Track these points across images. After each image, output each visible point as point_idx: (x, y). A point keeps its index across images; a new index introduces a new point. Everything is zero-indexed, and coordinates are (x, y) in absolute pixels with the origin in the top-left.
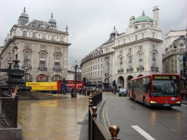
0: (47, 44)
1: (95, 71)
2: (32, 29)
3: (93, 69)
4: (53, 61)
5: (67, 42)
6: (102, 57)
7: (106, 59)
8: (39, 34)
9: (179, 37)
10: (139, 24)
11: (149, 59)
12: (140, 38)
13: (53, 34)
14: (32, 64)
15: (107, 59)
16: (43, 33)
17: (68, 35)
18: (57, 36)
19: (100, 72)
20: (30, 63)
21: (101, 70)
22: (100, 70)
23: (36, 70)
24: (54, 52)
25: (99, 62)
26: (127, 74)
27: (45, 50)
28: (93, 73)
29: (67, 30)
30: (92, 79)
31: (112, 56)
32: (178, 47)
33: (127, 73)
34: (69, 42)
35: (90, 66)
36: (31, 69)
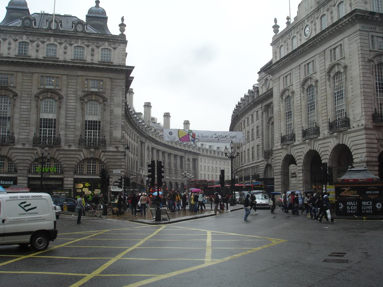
0: (62, 72)
4: (79, 118)
5: (121, 63)
8: (38, 46)
11: (364, 86)
14: (16, 131)
17: (125, 42)
18: (90, 48)
20: (12, 126)
23: (27, 146)
24: (80, 94)
26: (302, 146)
33: (304, 143)
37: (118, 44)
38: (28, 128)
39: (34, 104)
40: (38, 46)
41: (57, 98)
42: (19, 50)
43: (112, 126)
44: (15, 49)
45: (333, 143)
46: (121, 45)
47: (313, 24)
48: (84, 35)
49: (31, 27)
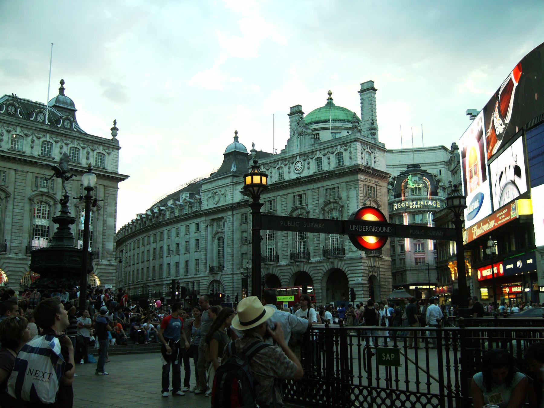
1: (173, 260)
2: (10, 124)
3: (165, 255)
5: (114, 170)
6: (198, 220)
7: (212, 225)
9: (406, 169)
10: (327, 128)
12: (329, 164)
13: (76, 142)
14: (8, 237)
15: (215, 224)
16: (43, 139)
17: (118, 148)
19: (192, 265)
21: (197, 255)
22: (193, 256)
23: (20, 256)
25: (187, 232)
27: (48, 193)
28: (165, 267)
29: (114, 135)
30: (162, 285)
31: (233, 215)
32: (406, 195)
34: (121, 171)
35: (153, 246)
36: (5, 251)
37: (111, 149)
38: (21, 235)
39: (27, 208)
40: (33, 141)
41: (52, 203)
42: (12, 144)
43: (105, 237)
44: (8, 142)
45: (327, 266)
46: (115, 150)
47: (306, 162)
48: (80, 136)
49: (16, 116)
